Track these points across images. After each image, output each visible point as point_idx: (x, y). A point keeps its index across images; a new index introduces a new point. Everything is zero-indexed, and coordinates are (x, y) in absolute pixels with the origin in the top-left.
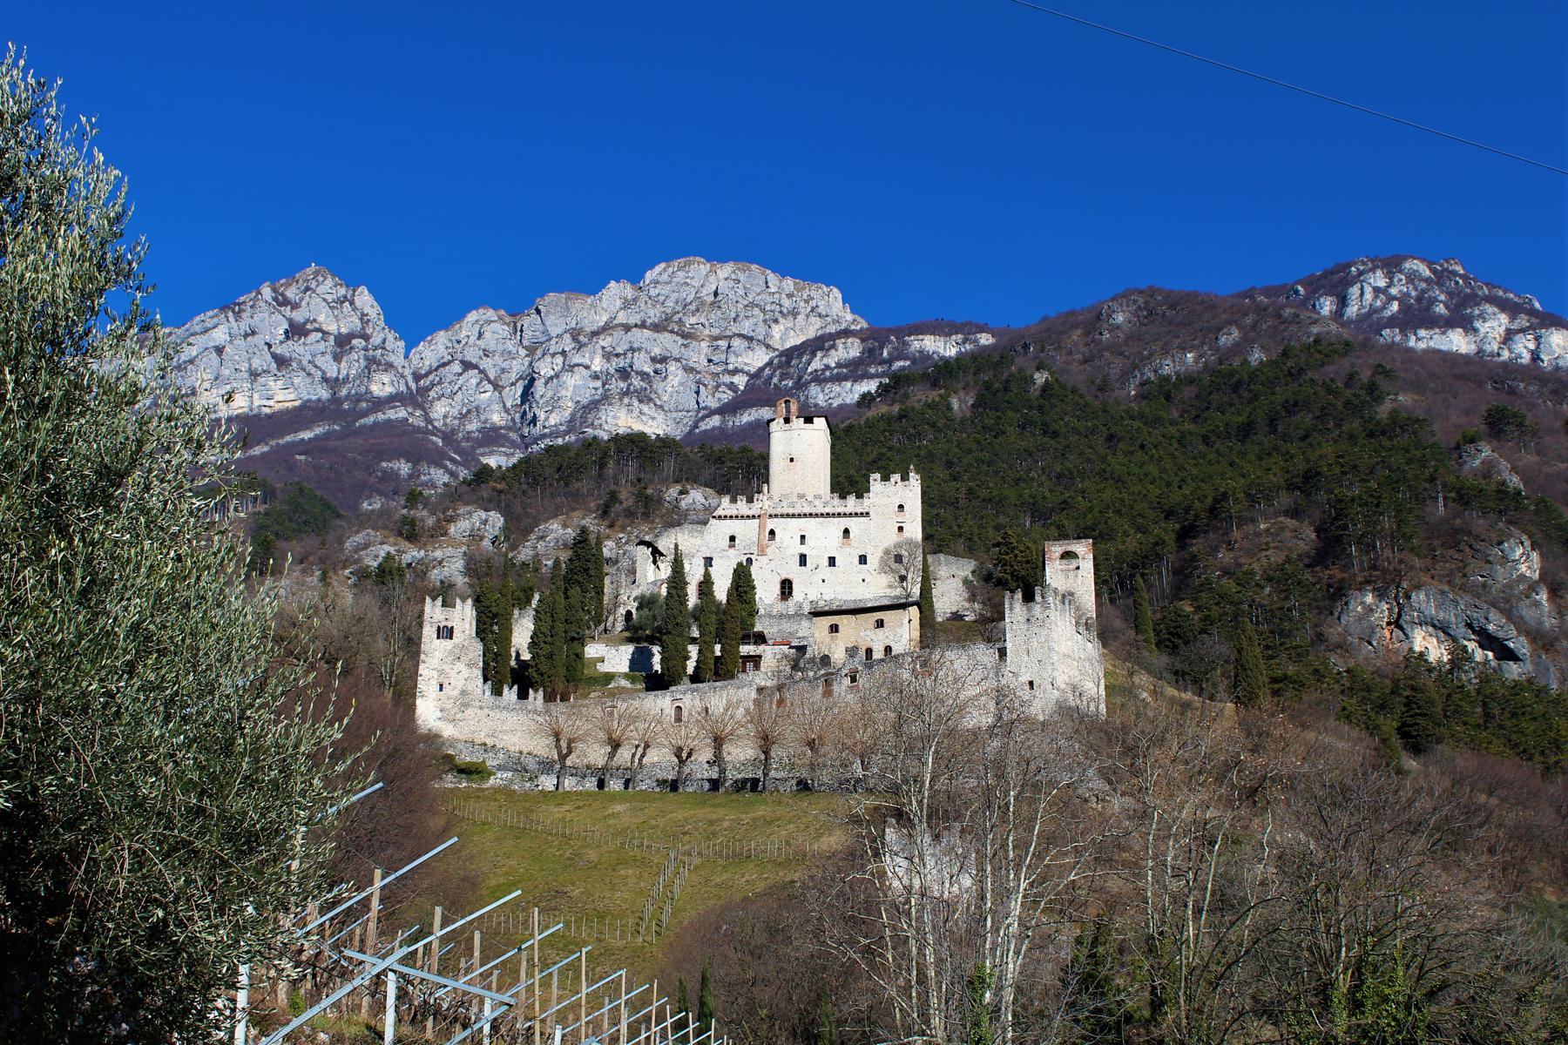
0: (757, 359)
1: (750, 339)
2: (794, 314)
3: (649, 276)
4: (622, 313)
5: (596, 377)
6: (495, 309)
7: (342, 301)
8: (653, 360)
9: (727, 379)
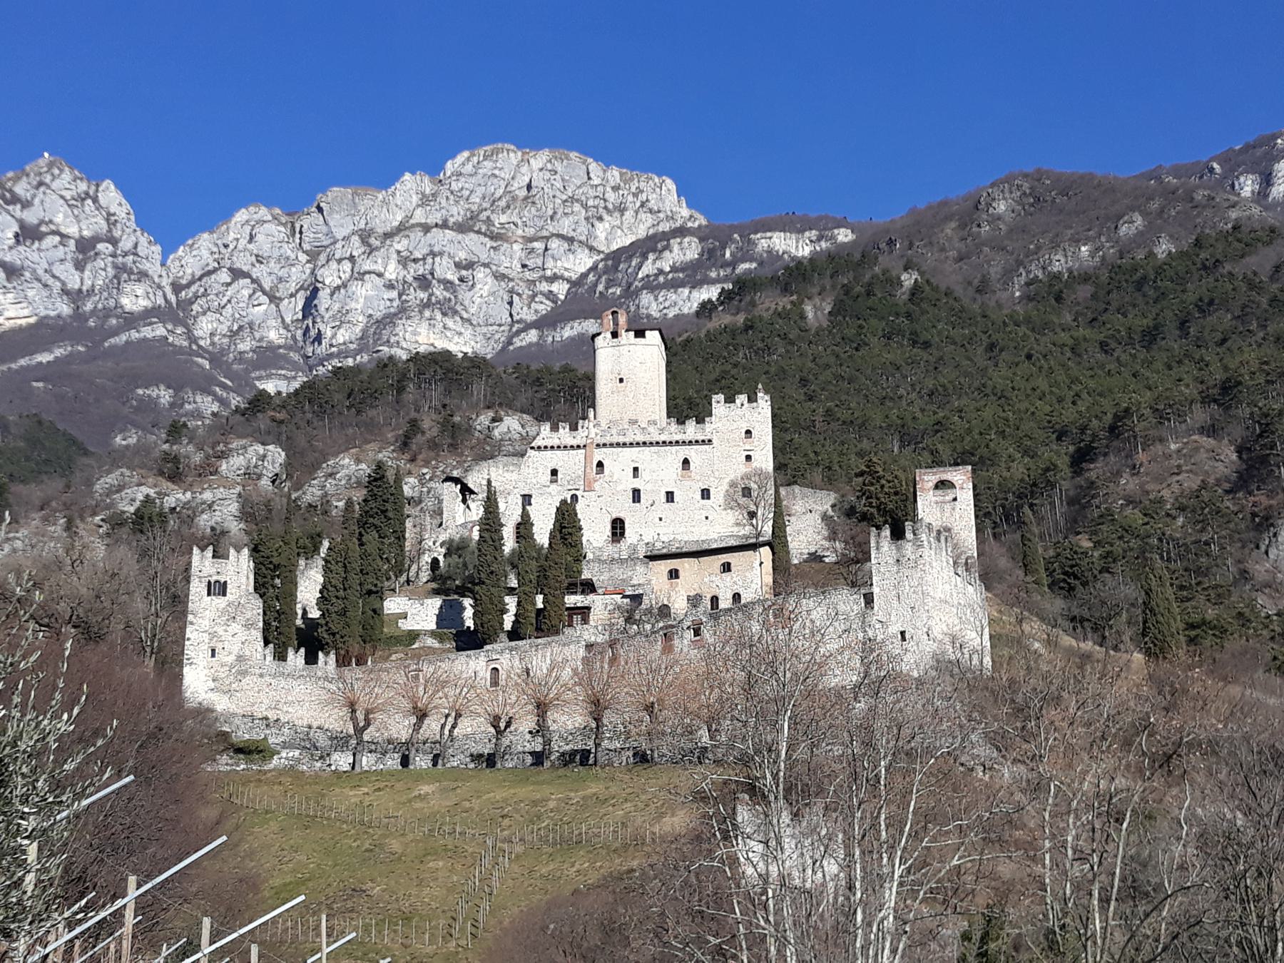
0: (580, 263)
1: (570, 240)
2: (621, 210)
3: (450, 166)
4: (419, 212)
5: (390, 286)
6: (269, 206)
7: (82, 198)
8: (458, 266)
9: (544, 287)
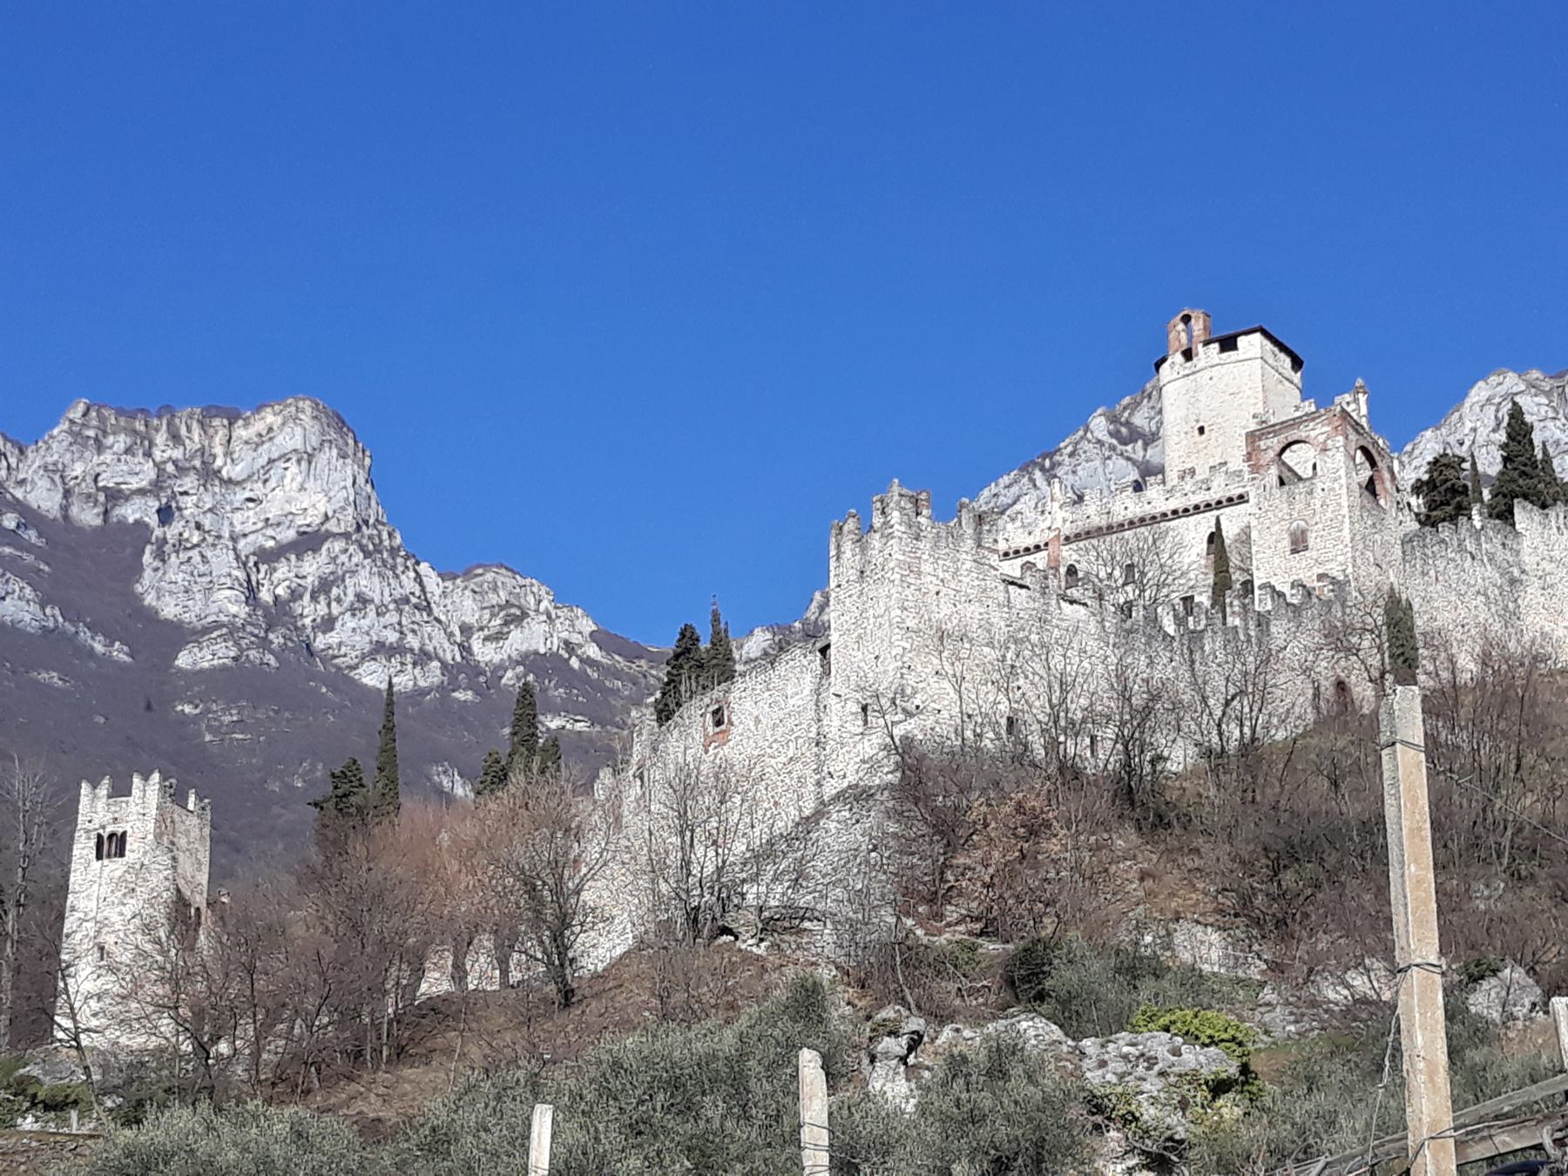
6: (1521, 371)
